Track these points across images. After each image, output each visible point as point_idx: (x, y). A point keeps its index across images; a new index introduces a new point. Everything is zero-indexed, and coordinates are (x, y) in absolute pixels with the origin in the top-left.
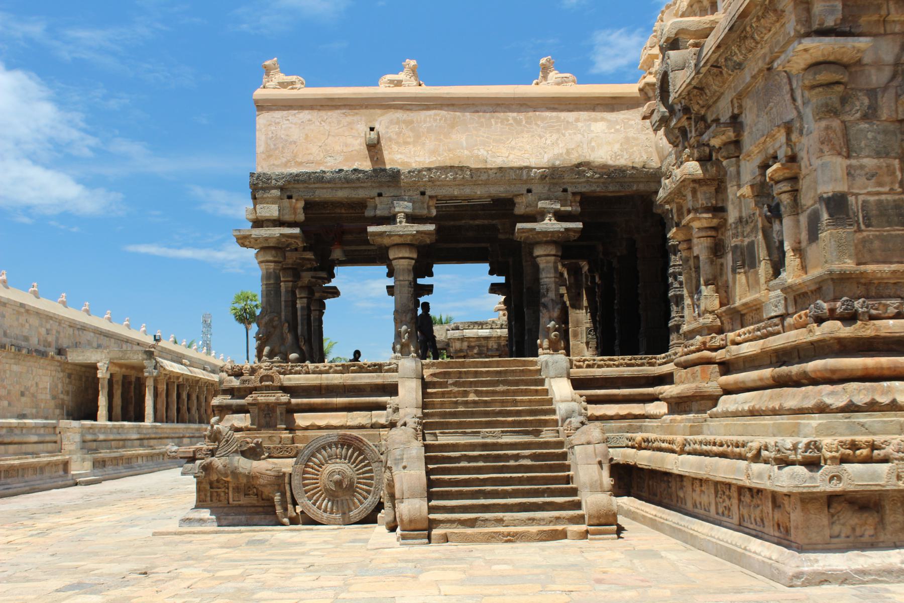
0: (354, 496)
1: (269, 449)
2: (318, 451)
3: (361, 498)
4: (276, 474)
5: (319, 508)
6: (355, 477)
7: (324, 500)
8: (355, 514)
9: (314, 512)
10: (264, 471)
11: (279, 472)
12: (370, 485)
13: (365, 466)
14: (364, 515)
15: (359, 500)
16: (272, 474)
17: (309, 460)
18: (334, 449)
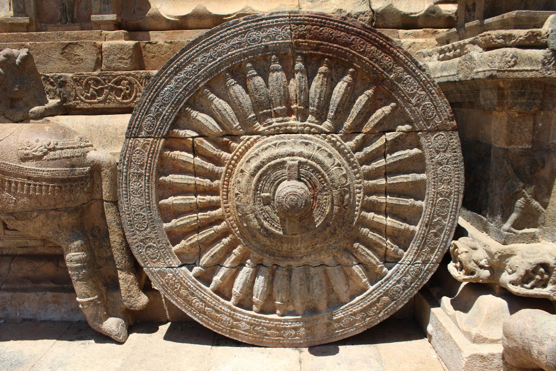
0: (350, 252)
1: (63, 84)
2: (215, 81)
3: (374, 259)
4: (60, 171)
5: (223, 292)
6: (358, 186)
7: (240, 265)
8: (352, 311)
9: (202, 301)
10: (15, 164)
11: (73, 162)
12: (410, 216)
13: (394, 145)
14: (383, 316)
15: (367, 268)
16: (45, 170)
17: (180, 119)
18: (277, 76)
